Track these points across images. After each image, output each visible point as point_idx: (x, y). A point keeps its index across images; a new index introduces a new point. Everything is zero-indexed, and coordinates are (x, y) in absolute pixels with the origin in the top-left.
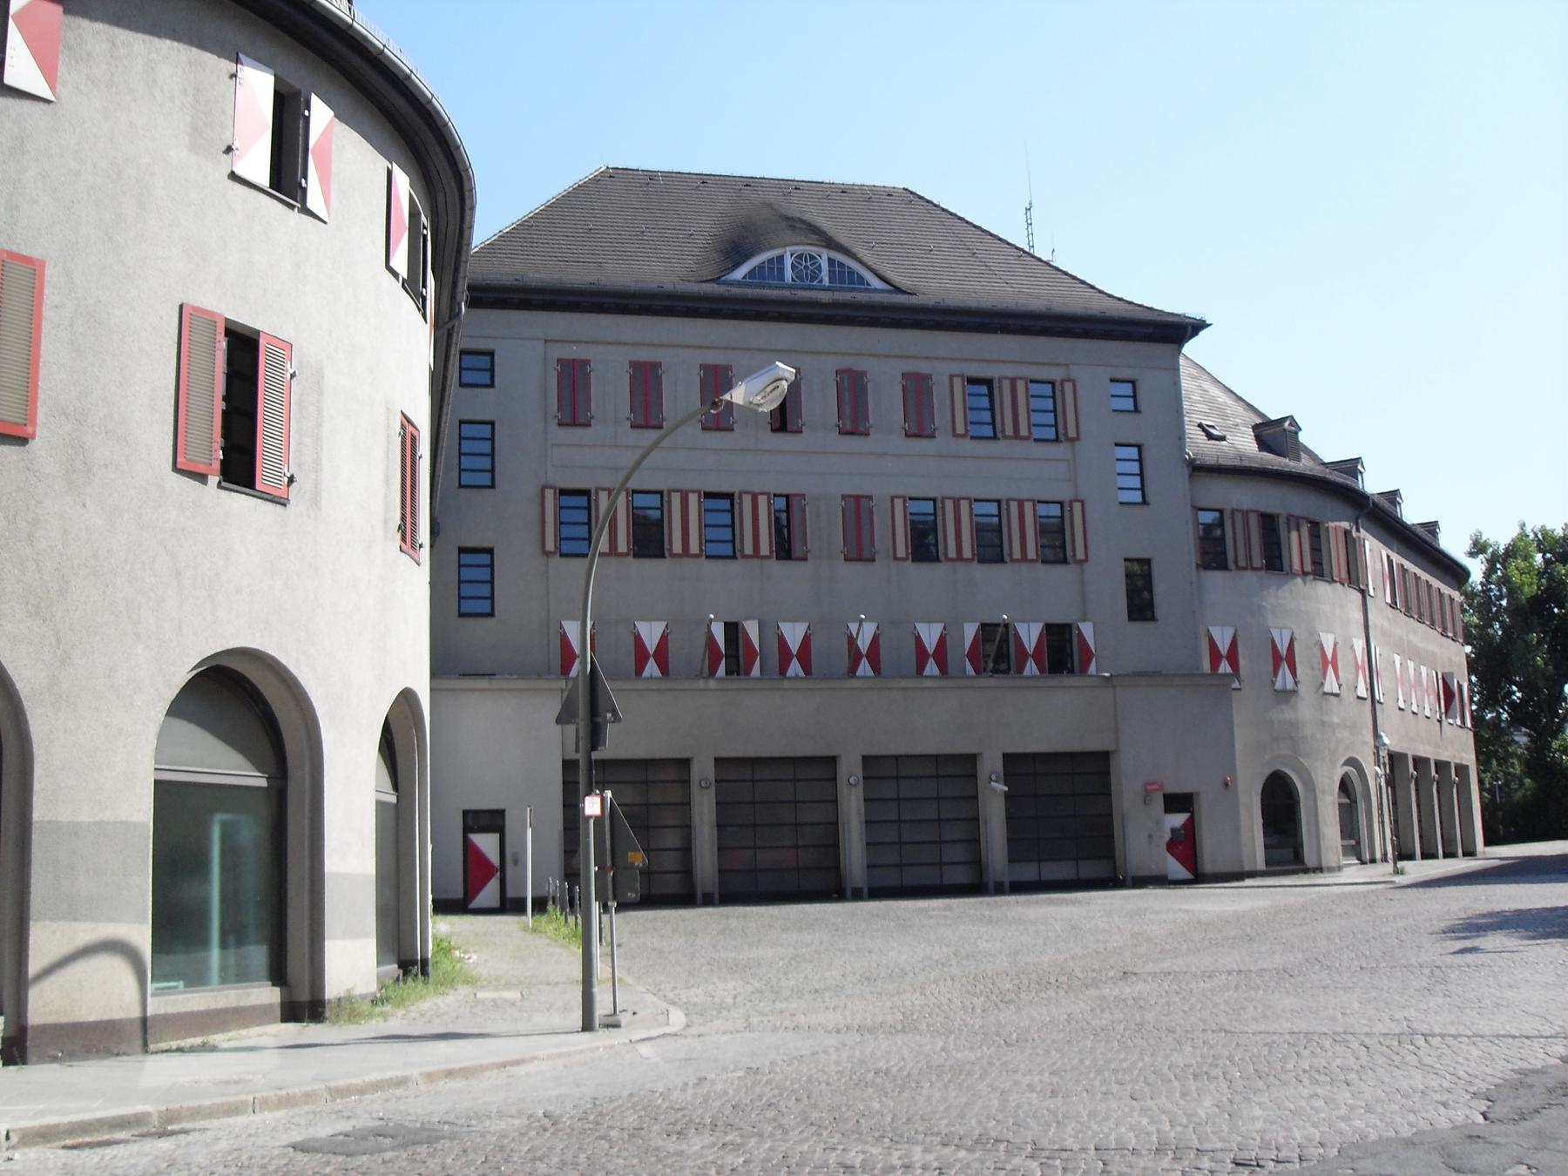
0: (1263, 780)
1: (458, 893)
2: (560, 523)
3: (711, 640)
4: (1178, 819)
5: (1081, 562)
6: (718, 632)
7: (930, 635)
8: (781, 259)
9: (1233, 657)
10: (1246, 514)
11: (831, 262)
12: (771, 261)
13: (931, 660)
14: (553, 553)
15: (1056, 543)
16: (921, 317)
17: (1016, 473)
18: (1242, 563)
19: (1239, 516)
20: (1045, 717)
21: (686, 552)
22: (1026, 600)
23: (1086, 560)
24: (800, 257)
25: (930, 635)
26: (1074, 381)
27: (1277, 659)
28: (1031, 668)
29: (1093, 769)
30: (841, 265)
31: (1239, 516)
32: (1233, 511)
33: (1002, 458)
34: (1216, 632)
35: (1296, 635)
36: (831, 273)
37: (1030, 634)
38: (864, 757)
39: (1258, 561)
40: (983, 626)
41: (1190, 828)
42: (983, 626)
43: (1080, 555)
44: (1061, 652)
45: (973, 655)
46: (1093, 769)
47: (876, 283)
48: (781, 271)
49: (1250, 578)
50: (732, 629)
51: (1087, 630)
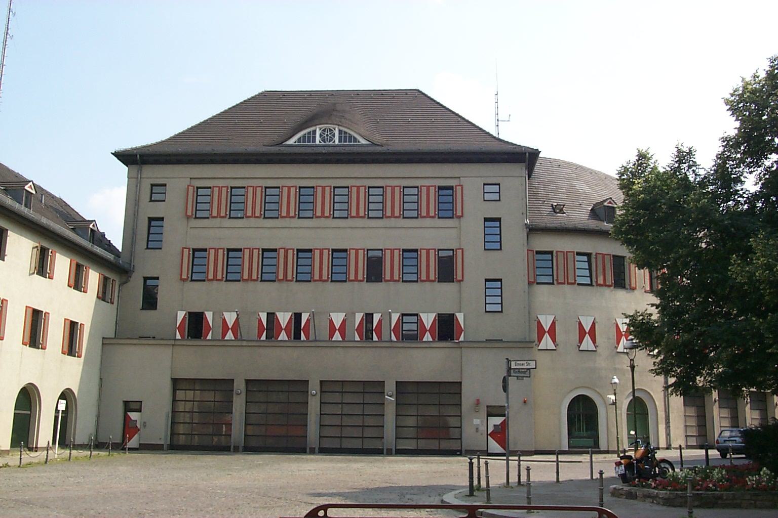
0: (21, 388)
1: (118, 440)
2: (242, 265)
3: (260, 321)
4: (498, 420)
5: (460, 281)
6: (264, 317)
7: (338, 319)
8: (314, 132)
9: (552, 332)
10: (604, 255)
11: (340, 132)
12: (309, 133)
13: (230, 331)
14: (283, 280)
15: (447, 269)
16: (329, 157)
17: (431, 236)
18: (561, 280)
19: (600, 257)
20: (427, 363)
21: (285, 278)
22: (428, 302)
23: (462, 280)
24: (324, 130)
25: (338, 319)
26: (462, 186)
27: (582, 333)
28: (428, 337)
29: (449, 392)
30: (345, 133)
31: (600, 257)
32: (557, 252)
33: (274, 228)
34: (542, 318)
35: (597, 320)
36: (340, 138)
37: (428, 319)
38: (397, 382)
39: (610, 279)
40: (191, 314)
41: (504, 426)
42: (191, 314)
43: (459, 278)
44: (446, 328)
45: (359, 330)
46: (449, 392)
47: (363, 142)
48: (314, 138)
49: (607, 291)
50: (271, 316)
51: (460, 317)
